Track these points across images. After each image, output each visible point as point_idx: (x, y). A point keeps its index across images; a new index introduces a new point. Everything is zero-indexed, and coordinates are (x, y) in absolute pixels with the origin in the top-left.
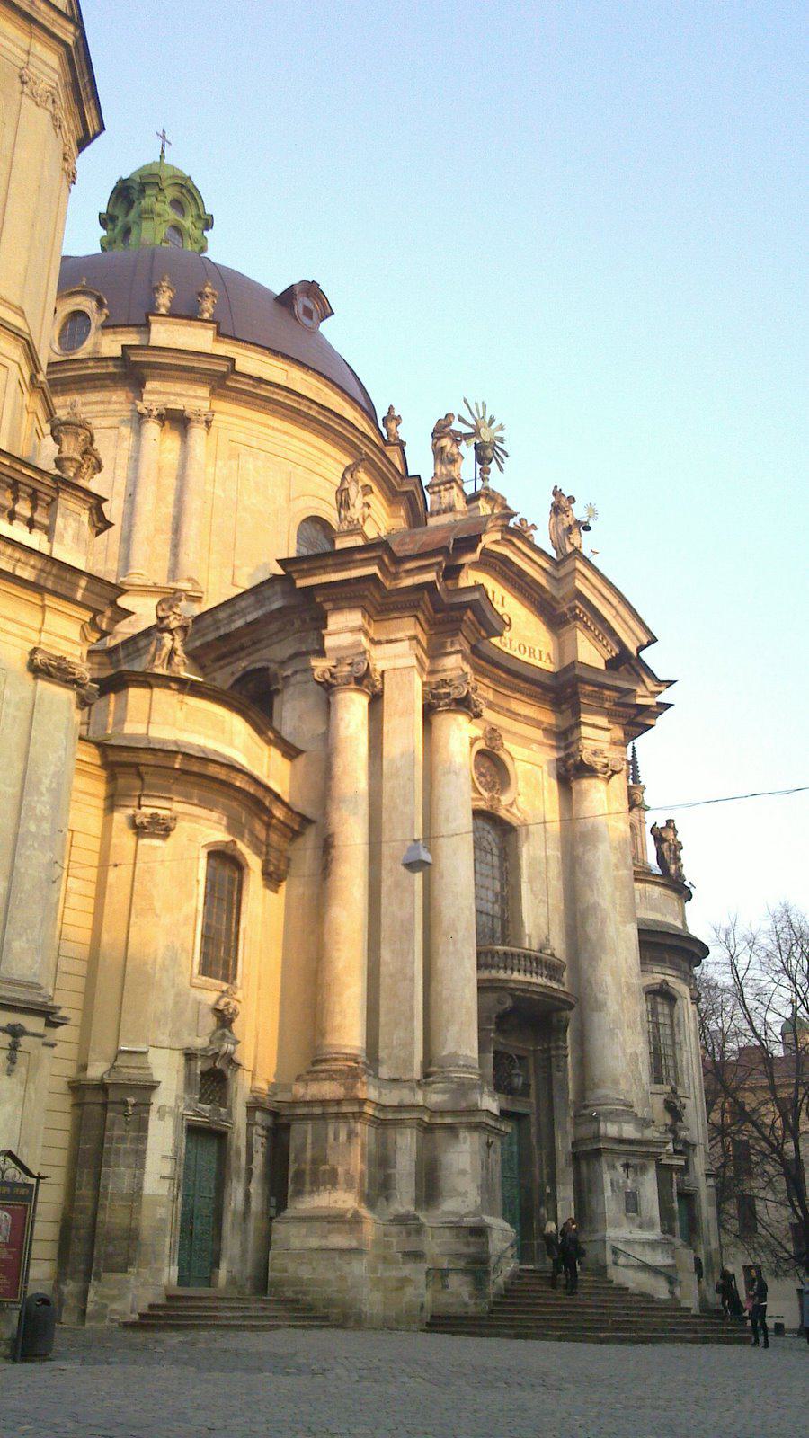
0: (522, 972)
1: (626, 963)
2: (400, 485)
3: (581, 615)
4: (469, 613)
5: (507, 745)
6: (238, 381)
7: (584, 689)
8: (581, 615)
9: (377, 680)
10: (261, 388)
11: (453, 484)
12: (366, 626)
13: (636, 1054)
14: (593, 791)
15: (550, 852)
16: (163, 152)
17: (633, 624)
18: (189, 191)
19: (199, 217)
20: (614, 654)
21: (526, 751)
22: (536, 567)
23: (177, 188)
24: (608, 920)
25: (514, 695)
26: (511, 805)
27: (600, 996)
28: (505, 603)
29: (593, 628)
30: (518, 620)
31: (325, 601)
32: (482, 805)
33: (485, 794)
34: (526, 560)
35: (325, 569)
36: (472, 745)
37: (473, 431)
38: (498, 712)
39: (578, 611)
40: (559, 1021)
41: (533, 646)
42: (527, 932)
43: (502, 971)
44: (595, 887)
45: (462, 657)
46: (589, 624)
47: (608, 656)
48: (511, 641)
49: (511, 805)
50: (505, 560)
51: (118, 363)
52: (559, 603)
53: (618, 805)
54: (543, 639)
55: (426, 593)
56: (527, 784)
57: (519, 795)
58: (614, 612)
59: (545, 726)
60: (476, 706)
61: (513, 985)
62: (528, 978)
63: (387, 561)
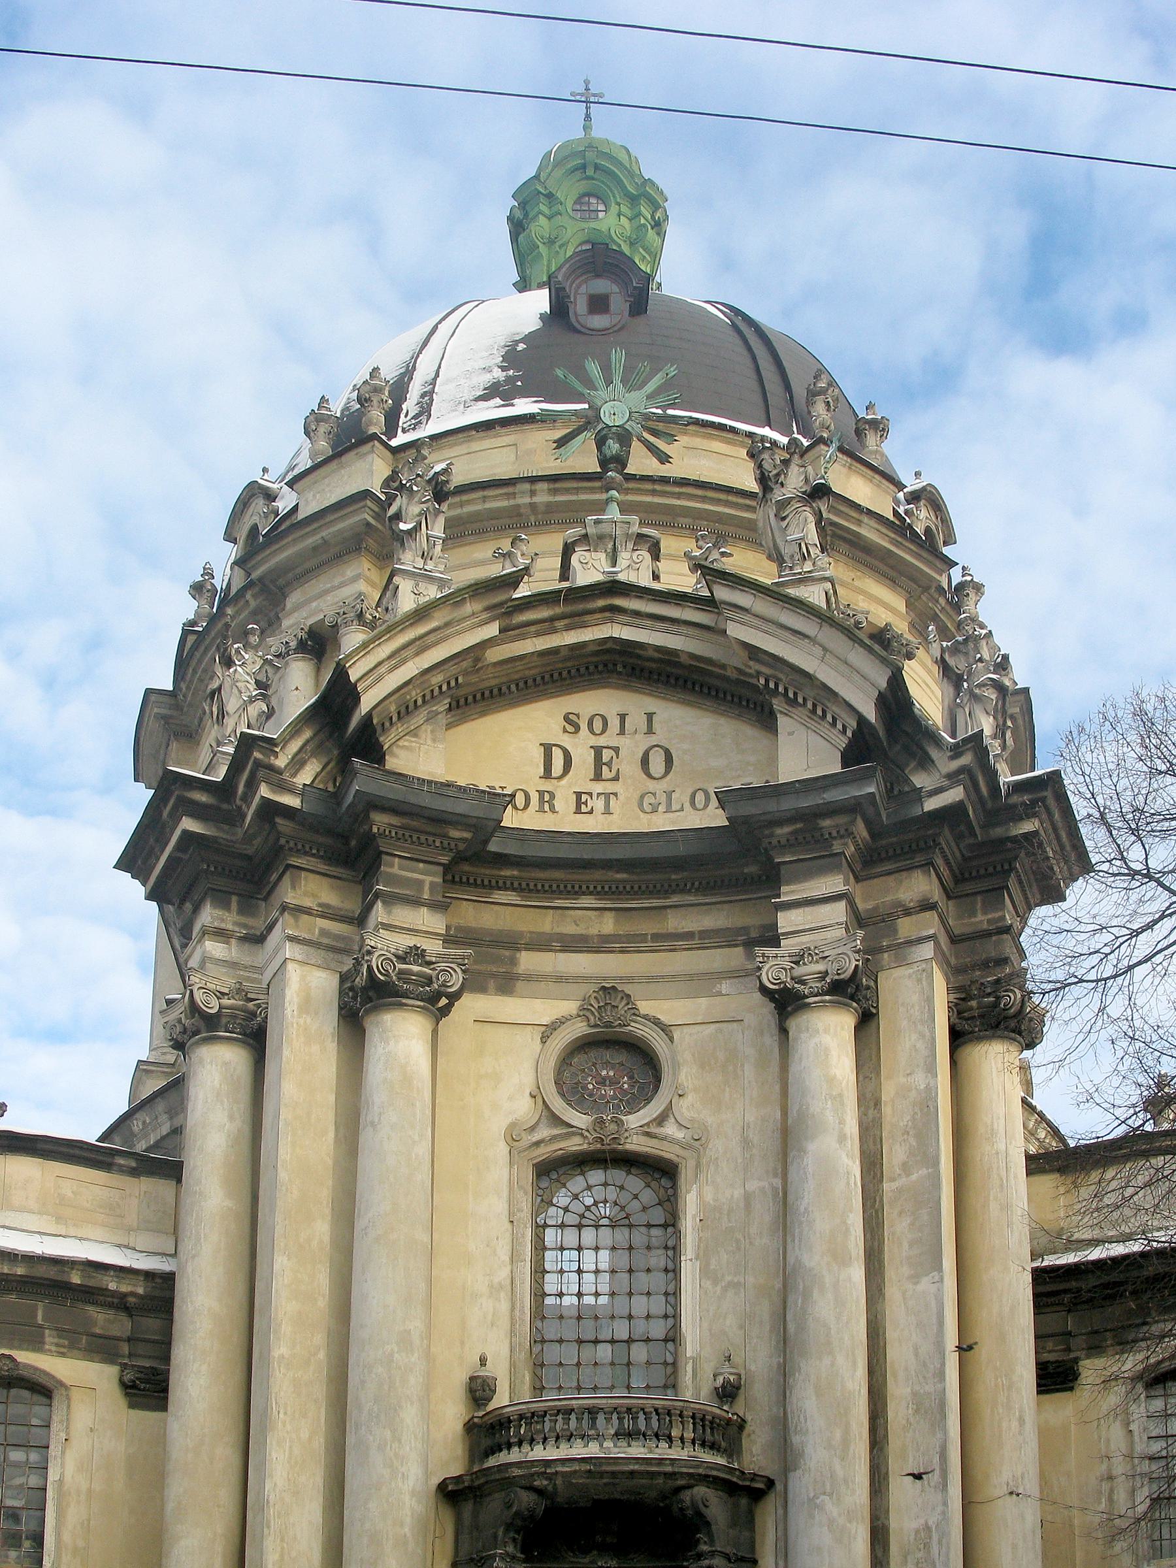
0: (552, 1441)
5: (644, 1007)
21: (703, 1002)
24: (816, 1294)
25: (668, 902)
27: (796, 1439)
28: (656, 725)
30: (685, 746)
31: (182, 902)
32: (575, 1145)
36: (544, 1039)
40: (681, 1509)
43: (516, 1449)
48: (669, 794)
50: (627, 649)
53: (914, 1037)
54: (752, 759)
59: (754, 934)
61: (517, 1472)
62: (564, 1451)
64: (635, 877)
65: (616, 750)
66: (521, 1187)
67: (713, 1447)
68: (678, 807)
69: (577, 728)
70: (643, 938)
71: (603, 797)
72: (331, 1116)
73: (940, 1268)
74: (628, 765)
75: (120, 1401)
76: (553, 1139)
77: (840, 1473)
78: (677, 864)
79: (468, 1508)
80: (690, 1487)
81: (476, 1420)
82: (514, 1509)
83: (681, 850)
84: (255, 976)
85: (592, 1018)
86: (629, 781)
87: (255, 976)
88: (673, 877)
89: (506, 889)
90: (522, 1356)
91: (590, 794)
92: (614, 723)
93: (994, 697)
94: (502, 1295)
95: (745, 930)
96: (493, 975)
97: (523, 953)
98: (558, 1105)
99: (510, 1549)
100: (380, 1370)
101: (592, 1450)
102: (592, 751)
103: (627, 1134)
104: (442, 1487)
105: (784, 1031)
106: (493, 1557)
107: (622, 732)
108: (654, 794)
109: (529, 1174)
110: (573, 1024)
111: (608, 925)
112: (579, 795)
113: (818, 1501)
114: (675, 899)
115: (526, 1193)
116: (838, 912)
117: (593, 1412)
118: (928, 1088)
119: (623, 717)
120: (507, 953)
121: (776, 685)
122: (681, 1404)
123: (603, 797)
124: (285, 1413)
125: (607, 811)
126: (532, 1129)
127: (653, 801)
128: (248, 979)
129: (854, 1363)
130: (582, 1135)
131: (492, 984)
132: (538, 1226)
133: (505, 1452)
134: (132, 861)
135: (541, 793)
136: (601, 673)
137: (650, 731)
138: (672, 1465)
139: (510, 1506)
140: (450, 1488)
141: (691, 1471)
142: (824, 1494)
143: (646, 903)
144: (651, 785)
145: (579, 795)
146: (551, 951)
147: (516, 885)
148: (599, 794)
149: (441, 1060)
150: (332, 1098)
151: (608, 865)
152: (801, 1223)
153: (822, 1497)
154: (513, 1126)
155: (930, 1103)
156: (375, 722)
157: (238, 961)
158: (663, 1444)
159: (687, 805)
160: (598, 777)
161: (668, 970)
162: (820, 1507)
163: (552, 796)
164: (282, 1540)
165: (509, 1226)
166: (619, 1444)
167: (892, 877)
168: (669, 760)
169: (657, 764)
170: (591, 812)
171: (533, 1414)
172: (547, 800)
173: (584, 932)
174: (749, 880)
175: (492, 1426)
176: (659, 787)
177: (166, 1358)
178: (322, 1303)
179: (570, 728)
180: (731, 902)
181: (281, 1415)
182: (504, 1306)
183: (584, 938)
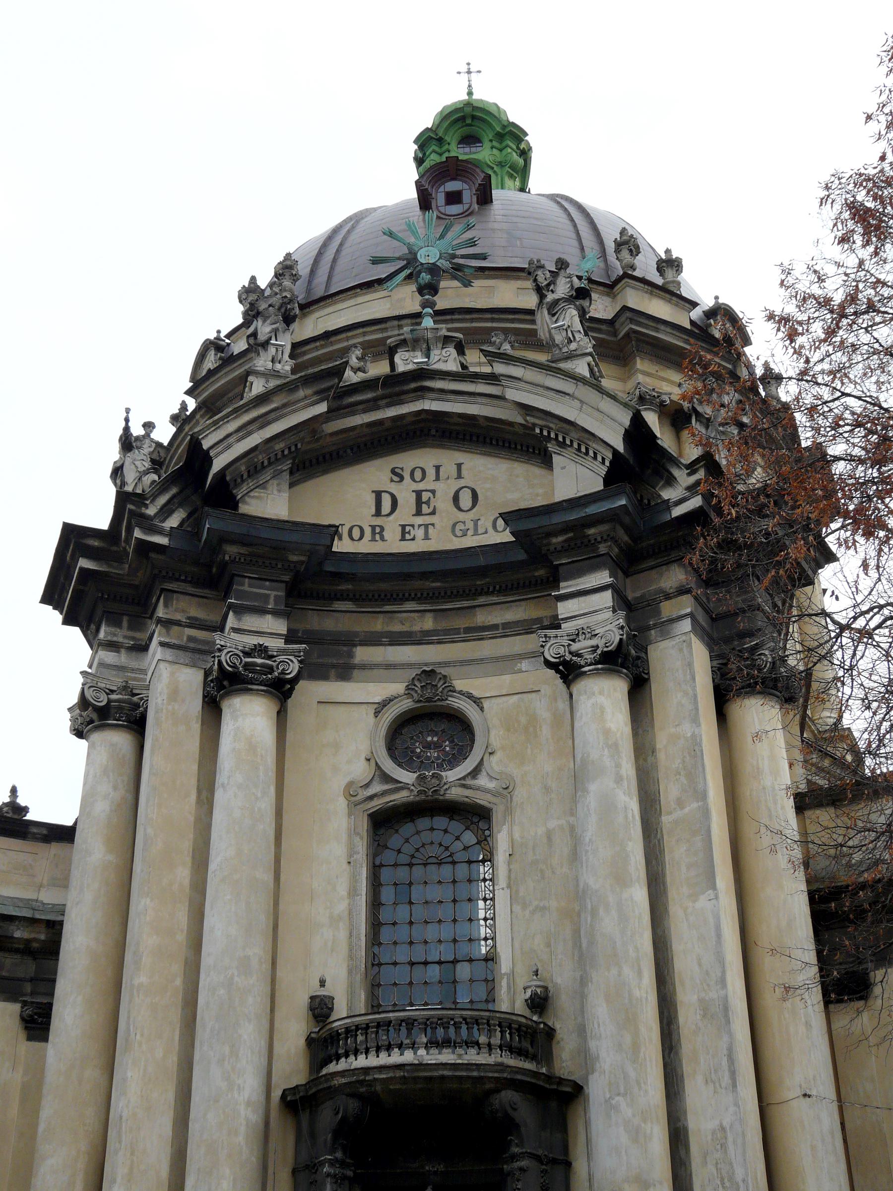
0: (373, 1053)
1: (700, 965)
2: (615, 334)
3: (545, 433)
4: (231, 550)
5: (459, 684)
6: (305, 353)
7: (549, 544)
8: (545, 433)
9: (142, 699)
10: (332, 344)
11: (250, 378)
12: (120, 635)
13: (723, 1129)
14: (583, 698)
15: (552, 824)
16: (470, 86)
17: (606, 404)
18: (474, 117)
19: (500, 137)
20: (607, 463)
21: (507, 678)
22: (479, 399)
23: (460, 124)
24: (601, 912)
25: (476, 603)
26: (475, 773)
27: (592, 1044)
28: (464, 472)
29: (568, 442)
30: (488, 486)
32: (402, 796)
33: (407, 777)
35: (64, 590)
36: (377, 713)
37: (405, 262)
38: (440, 642)
39: (538, 431)
42: (503, 972)
43: (343, 1059)
44: (584, 858)
45: (234, 612)
46: (561, 439)
47: (603, 470)
48: (476, 522)
49: (475, 773)
51: (203, 411)
53: (679, 695)
54: (541, 491)
55: (153, 555)
56: (509, 730)
57: (490, 754)
58: (577, 403)
59: (546, 623)
60: (271, 669)
62: (384, 1059)
63: (96, 543)
64: (446, 585)
65: (433, 492)
66: (358, 834)
67: (520, 1052)
68: (484, 531)
69: (402, 478)
70: (457, 631)
71: (423, 527)
72: (194, 782)
73: (714, 887)
74: (443, 502)
75: (22, 1035)
76: (384, 793)
77: (632, 1074)
78: (482, 571)
79: (305, 1118)
80: (498, 1091)
81: (313, 1035)
82: (340, 1115)
83: (482, 561)
84: (142, 676)
85: (415, 695)
87: (142, 676)
88: (478, 583)
89: (344, 600)
90: (359, 977)
91: (413, 526)
92: (431, 473)
93: (736, 432)
94: (341, 924)
95: (539, 620)
96: (334, 666)
97: (359, 648)
98: (389, 766)
99: (339, 1155)
100: (222, 992)
101: (408, 1057)
102: (414, 494)
103: (445, 787)
104: (283, 1096)
105: (571, 696)
106: (322, 1164)
107: (438, 478)
108: (464, 523)
109: (364, 824)
110: (401, 701)
111: (428, 623)
112: (403, 527)
113: (613, 1102)
114: (482, 600)
115: (362, 838)
116: (608, 594)
117: (410, 1023)
118: (693, 735)
119: (438, 468)
120: (345, 649)
122: (487, 1014)
123: (423, 527)
124: (142, 1035)
125: (427, 537)
126: (367, 786)
127: (462, 527)
128: (135, 679)
129: (640, 973)
130: (409, 789)
131: (333, 673)
132: (374, 866)
133: (334, 1062)
134: (51, 597)
135: (373, 527)
137: (459, 476)
138: (478, 1070)
139: (337, 1113)
140: (289, 1098)
141: (496, 1075)
142: (619, 1094)
143: (458, 605)
144: (461, 516)
145: (403, 527)
146: (381, 645)
147: (351, 595)
148: (420, 526)
149: (290, 736)
150: (195, 767)
151: (424, 576)
152: (587, 851)
153: (617, 1098)
154: (350, 784)
155: (696, 748)
157: (127, 665)
158: (473, 1051)
159: (490, 530)
160: (419, 513)
161: (477, 655)
162: (616, 1108)
163: (382, 529)
164: (132, 1154)
165: (345, 865)
166: (432, 1051)
167: (654, 572)
169: (466, 500)
170: (413, 539)
171: (357, 1027)
172: (378, 532)
173: (408, 630)
174: (539, 582)
175: (325, 1040)
176: (468, 517)
177: (52, 994)
178: (181, 937)
179: (396, 478)
180: (526, 599)
181: (138, 1037)
182: (342, 935)
183: (409, 634)
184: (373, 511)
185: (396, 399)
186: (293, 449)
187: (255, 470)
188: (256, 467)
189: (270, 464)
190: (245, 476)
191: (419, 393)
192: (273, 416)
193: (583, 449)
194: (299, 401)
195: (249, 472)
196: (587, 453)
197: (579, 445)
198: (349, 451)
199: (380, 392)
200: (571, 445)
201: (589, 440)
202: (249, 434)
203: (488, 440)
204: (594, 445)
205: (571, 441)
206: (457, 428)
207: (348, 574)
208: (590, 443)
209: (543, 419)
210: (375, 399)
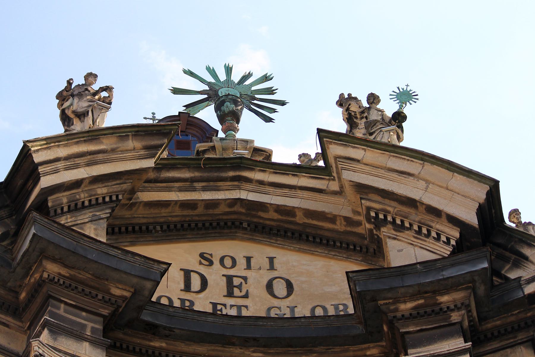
20: (453, 242)
29: (407, 225)
30: (303, 279)
34: (279, 191)
39: (373, 214)
41: (345, 302)
46: (398, 222)
48: (292, 309)
52: (359, 224)
58: (422, 184)
69: (211, 263)
71: (235, 308)
86: (257, 299)
91: (225, 305)
92: (242, 263)
102: (224, 279)
107: (249, 267)
108: (279, 308)
112: (215, 305)
119: (248, 259)
121: (385, 216)
123: (235, 308)
127: (278, 312)
135: (183, 301)
136: (230, 228)
137: (272, 267)
144: (276, 302)
145: (215, 305)
148: (232, 306)
156: (50, 204)
160: (230, 294)
163: (192, 303)
168: (290, 286)
169: (280, 288)
184: (182, 286)
185: (211, 184)
186: (114, 198)
187: (76, 208)
188: (76, 205)
189: (91, 205)
190: (66, 209)
191: (236, 183)
192: (100, 156)
193: (424, 231)
194: (127, 151)
195: (69, 207)
196: (428, 235)
197: (420, 228)
198: (158, 228)
199: (197, 174)
200: (411, 228)
201: (432, 221)
202: (76, 167)
203: (304, 237)
204: (438, 226)
205: (411, 225)
206: (272, 223)
207: (165, 328)
208: (433, 225)
209: (379, 203)
210: (192, 180)
